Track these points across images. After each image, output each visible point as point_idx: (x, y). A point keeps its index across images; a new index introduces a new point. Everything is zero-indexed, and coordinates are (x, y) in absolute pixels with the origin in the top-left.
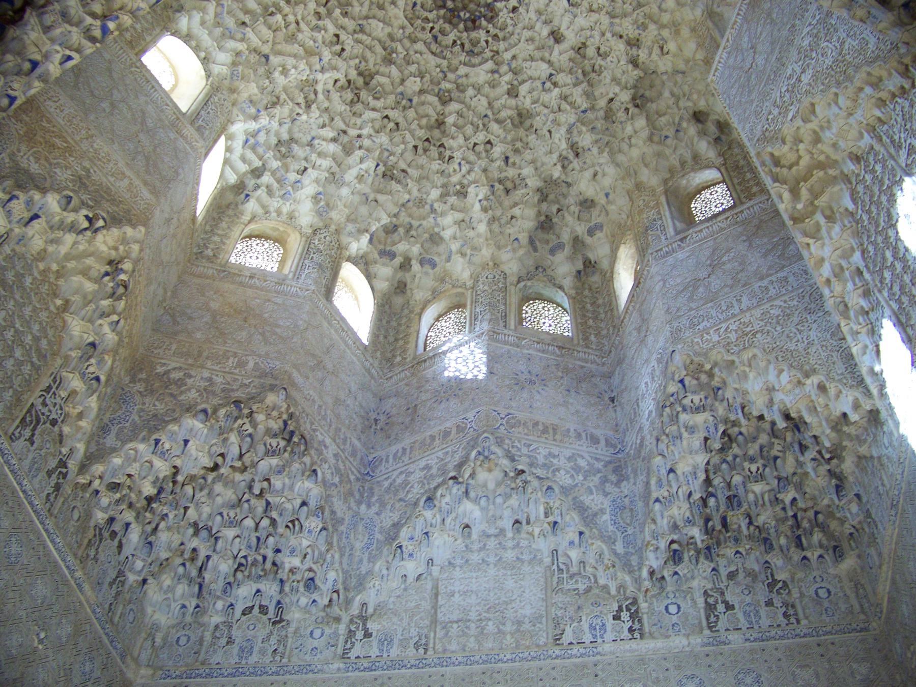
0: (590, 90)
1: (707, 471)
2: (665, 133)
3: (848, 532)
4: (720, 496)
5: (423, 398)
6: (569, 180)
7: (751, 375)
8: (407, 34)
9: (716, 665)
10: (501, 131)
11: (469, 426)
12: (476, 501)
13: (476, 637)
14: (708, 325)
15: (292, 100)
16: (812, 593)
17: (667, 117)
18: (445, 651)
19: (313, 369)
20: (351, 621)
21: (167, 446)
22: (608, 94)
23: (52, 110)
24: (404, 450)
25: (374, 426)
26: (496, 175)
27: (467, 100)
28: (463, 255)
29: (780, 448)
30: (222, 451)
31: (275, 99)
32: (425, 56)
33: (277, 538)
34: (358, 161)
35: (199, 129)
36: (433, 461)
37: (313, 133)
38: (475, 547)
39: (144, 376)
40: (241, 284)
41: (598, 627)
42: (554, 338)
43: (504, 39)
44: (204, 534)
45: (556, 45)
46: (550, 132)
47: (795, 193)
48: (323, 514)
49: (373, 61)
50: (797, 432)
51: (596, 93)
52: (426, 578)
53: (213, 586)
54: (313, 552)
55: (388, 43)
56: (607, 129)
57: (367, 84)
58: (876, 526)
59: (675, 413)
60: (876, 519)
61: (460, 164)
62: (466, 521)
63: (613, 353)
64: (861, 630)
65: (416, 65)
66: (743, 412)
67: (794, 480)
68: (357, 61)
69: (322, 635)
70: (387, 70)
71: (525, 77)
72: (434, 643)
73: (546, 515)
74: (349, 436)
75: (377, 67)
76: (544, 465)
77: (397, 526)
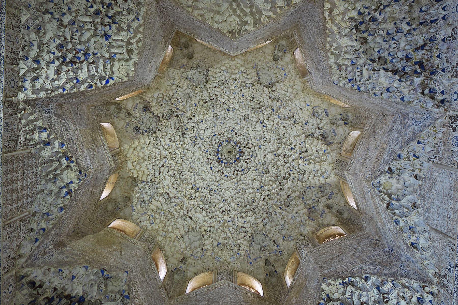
2: (283, 76)
6: (304, 122)
8: (236, 182)
12: (404, 195)
15: (241, 238)
19: (331, 263)
27: (269, 161)
31: (238, 246)
43: (248, 140)
46: (284, 127)
47: (246, 23)
49: (239, 198)
51: (267, 104)
61: (291, 170)
62: (410, 204)
68: (236, 206)
73: (410, 160)
74: (369, 255)
75: (245, 198)
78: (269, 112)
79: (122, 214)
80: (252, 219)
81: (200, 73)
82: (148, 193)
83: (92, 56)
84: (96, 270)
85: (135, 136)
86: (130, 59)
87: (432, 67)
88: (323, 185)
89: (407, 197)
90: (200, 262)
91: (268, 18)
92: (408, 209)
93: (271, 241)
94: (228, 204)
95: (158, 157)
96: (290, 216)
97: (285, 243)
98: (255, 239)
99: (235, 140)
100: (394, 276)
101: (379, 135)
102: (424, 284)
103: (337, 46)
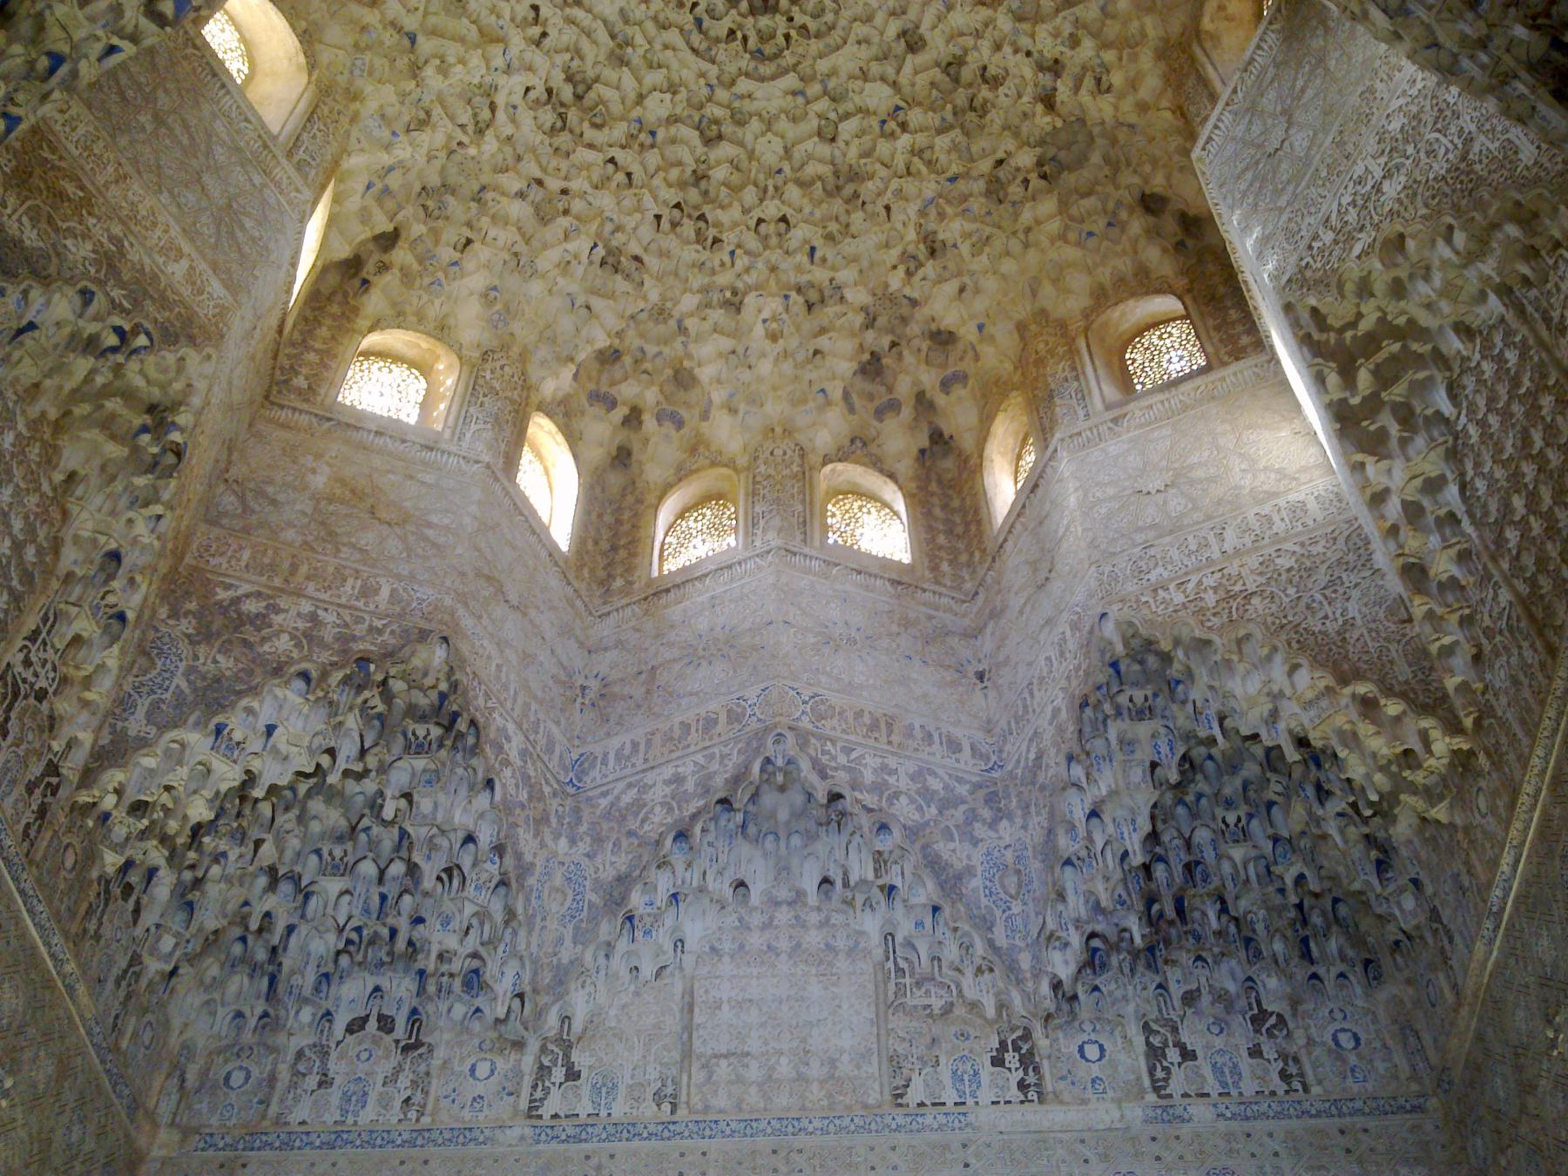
1: (1153, 818)
2: (1086, 227)
3: (1392, 938)
5: (668, 656)
6: (915, 295)
7: (1241, 668)
8: (651, 13)
9: (1169, 1157)
10: (806, 201)
11: (749, 711)
13: (760, 1085)
14: (1166, 574)
15: (452, 118)
16: (1328, 1038)
17: (1093, 199)
18: (707, 1109)
20: (543, 1049)
21: (238, 736)
22: (994, 152)
23: (58, 128)
24: (635, 745)
25: (579, 700)
26: (793, 278)
27: (749, 138)
28: (733, 411)
29: (1279, 788)
30: (332, 744)
31: (422, 115)
32: (680, 54)
33: (418, 897)
34: (562, 236)
35: (300, 167)
36: (687, 769)
37: (486, 178)
38: (756, 919)
39: (192, 605)
41: (966, 1077)
42: (886, 563)
43: (818, 36)
44: (286, 888)
45: (909, 56)
46: (888, 208)
49: (594, 55)
50: (1313, 768)
51: (975, 149)
52: (672, 974)
53: (297, 980)
54: (482, 924)
55: (619, 26)
56: (989, 213)
57: (579, 97)
58: (1451, 940)
59: (1100, 717)
60: (1452, 927)
61: (732, 253)
63: (981, 597)
64: (1415, 1109)
65: (664, 70)
66: (1221, 725)
67: (1302, 844)
68: (567, 56)
69: (492, 1072)
71: (849, 107)
72: (688, 1095)
74: (541, 716)
75: (598, 68)
76: (878, 788)
77: (624, 881)
78: (943, 158)
94: (571, 21)
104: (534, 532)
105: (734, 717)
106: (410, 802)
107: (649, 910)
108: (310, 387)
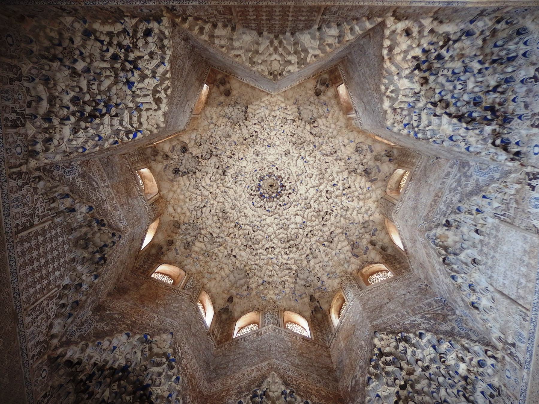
0: (307, 142)
2: (326, 111)
4: (472, 110)
6: (347, 158)
12: (462, 249)
13: (528, 281)
15: (286, 275)
17: (320, 108)
19: (380, 311)
20: (506, 350)
24: (435, 278)
27: (311, 196)
36: (437, 267)
40: (342, 327)
41: (536, 203)
46: (326, 163)
47: (289, 62)
48: (442, 339)
51: (308, 140)
54: (461, 353)
55: (280, 226)
57: (294, 240)
62: (470, 260)
68: (279, 242)
70: (290, 229)
73: (472, 214)
74: (420, 305)
75: (288, 233)
77: (463, 300)
78: (311, 148)
79: (165, 258)
80: (296, 256)
81: (239, 110)
82: (192, 234)
83: (114, 109)
84: (138, 337)
85: (175, 178)
86: (159, 108)
87: (505, 112)
88: (366, 222)
89: (466, 251)
90: (246, 300)
91: (315, 56)
92: (466, 264)
93: (316, 277)
94: (272, 240)
95: (199, 198)
96: (334, 253)
97: (330, 281)
98: (299, 275)
99: (276, 175)
100: (450, 335)
101: (431, 180)
102: (487, 348)
103: (393, 88)
104: (379, 287)
105: (425, 247)
106: (420, 360)
107: (471, 296)
108: (332, 335)
